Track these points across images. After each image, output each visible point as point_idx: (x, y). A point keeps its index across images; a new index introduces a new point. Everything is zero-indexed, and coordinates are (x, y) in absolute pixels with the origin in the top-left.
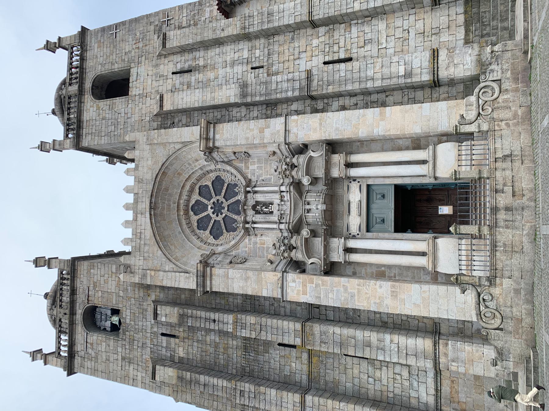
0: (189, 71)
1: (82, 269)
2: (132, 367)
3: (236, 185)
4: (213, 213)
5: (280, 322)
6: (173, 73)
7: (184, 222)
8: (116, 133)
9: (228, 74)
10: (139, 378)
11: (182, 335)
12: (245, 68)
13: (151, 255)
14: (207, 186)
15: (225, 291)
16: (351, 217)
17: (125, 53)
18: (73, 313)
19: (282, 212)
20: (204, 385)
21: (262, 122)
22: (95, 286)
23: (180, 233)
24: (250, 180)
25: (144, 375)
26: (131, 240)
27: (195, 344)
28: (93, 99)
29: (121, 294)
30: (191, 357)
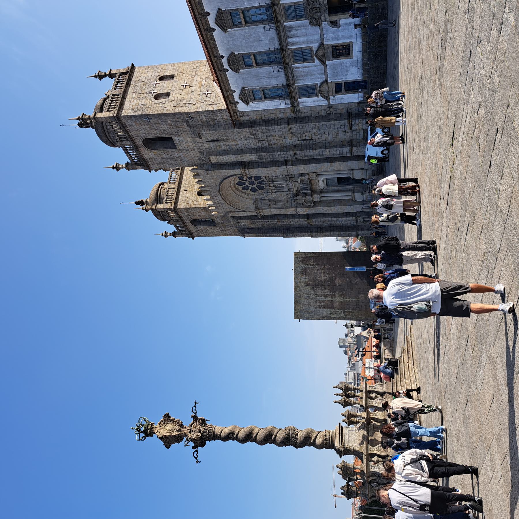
0: (218, 141)
2: (227, 232)
4: (250, 185)
5: (298, 220)
6: (206, 141)
7: (236, 191)
9: (244, 143)
12: (254, 141)
16: (320, 185)
17: (163, 129)
18: (184, 223)
19: (289, 188)
21: (274, 168)
23: (236, 196)
24: (268, 177)
26: (213, 204)
30: (257, 226)
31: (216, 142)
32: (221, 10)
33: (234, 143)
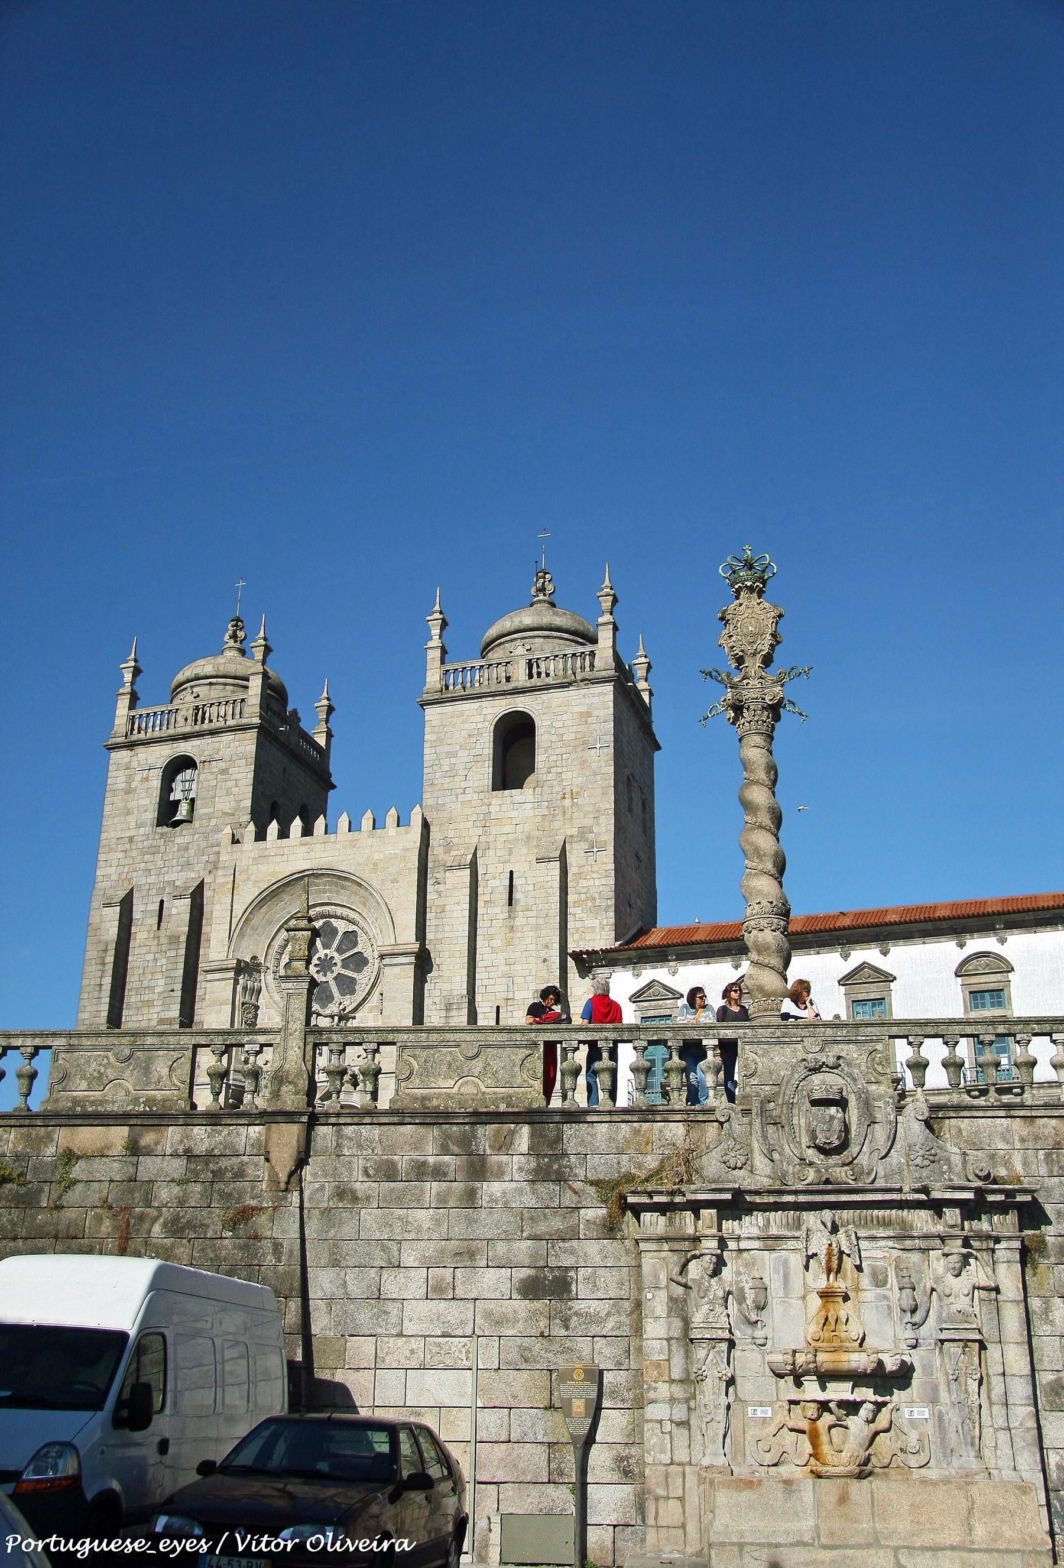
1: (245, 743)
2: (121, 855)
3: (352, 992)
6: (511, 873)
8: (438, 775)
9: (495, 969)
10: (111, 871)
11: (162, 933)
13: (253, 878)
14: (356, 944)
15: (207, 1002)
18: (186, 737)
20: (101, 985)
22: (224, 771)
25: (113, 877)
27: (150, 957)
28: (497, 718)
29: (213, 822)
31: (506, 896)
32: (892, 981)
33: (497, 943)
